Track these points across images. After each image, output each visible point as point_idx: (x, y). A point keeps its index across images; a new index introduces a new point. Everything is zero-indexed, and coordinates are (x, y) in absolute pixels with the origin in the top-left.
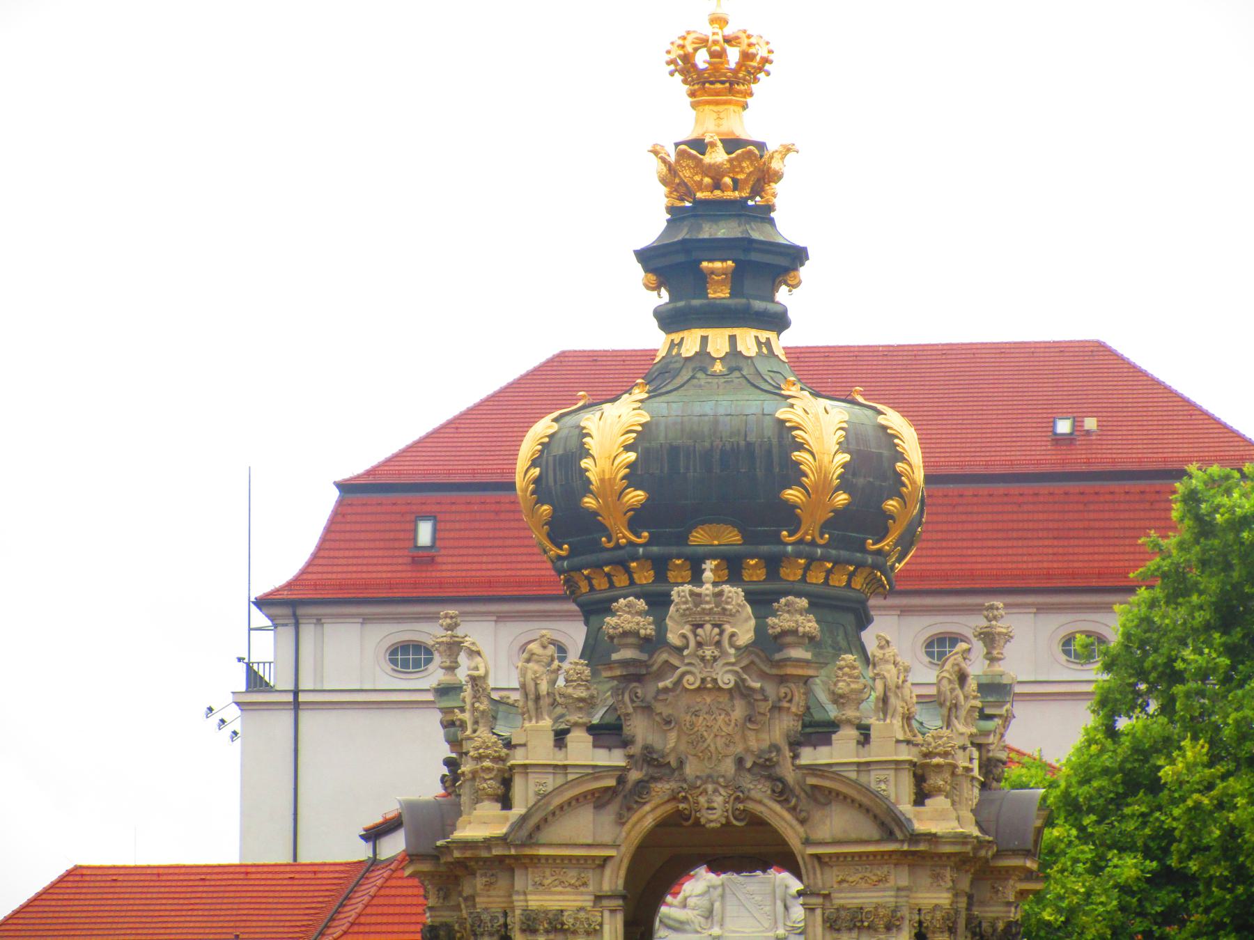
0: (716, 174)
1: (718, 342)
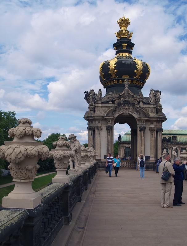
0: (124, 34)
1: (124, 54)
